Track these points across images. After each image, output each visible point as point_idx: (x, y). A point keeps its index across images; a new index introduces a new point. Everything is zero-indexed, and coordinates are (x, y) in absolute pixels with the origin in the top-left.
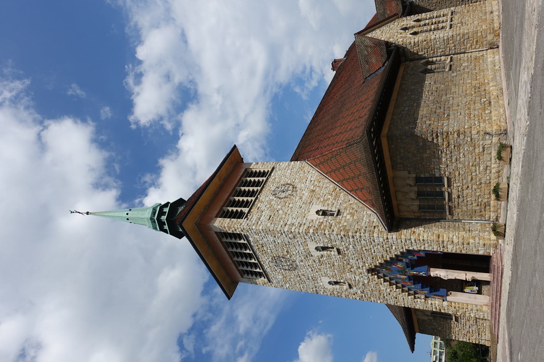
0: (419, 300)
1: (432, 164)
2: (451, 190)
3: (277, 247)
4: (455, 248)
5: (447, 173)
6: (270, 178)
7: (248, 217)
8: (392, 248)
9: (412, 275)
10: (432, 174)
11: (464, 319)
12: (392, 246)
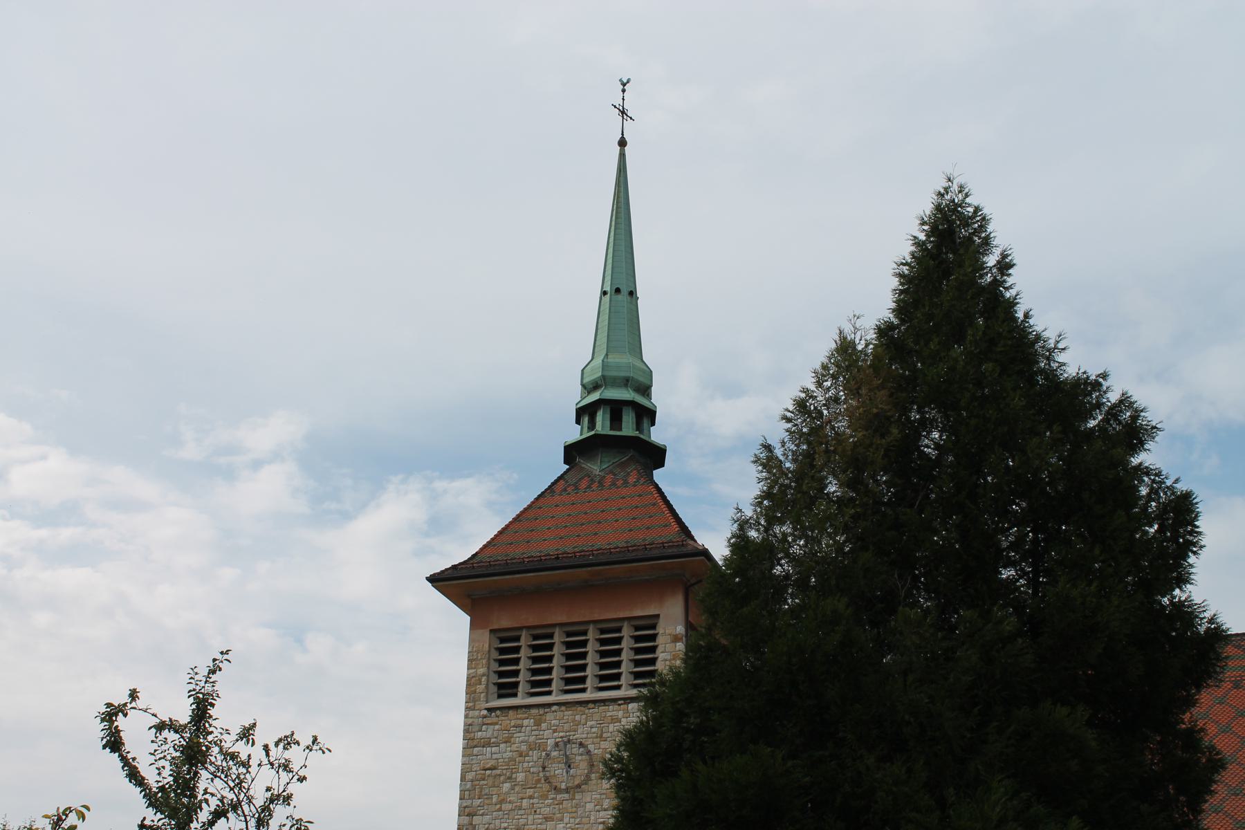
6: (619, 705)
7: (493, 714)
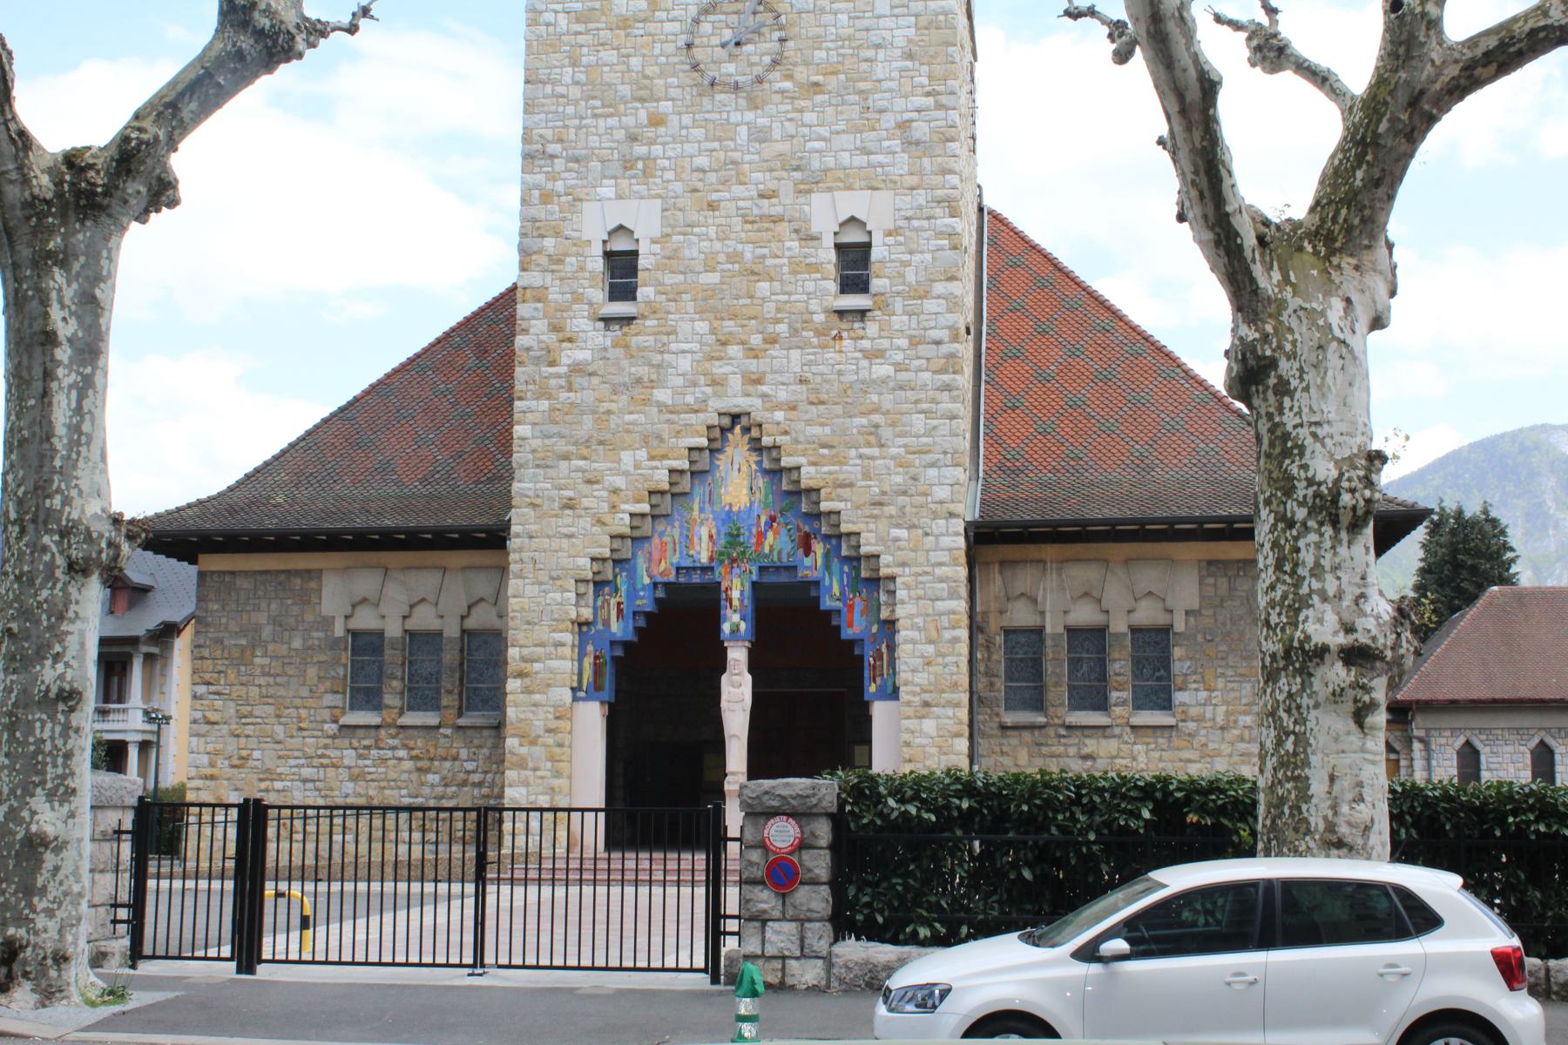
0: (572, 595)
1: (1230, 685)
2: (1114, 736)
3: (842, 47)
4: (924, 741)
5: (1191, 726)
8: (898, 526)
9: (719, 583)
10: (1185, 682)
11: (368, 762)
12: (912, 527)
